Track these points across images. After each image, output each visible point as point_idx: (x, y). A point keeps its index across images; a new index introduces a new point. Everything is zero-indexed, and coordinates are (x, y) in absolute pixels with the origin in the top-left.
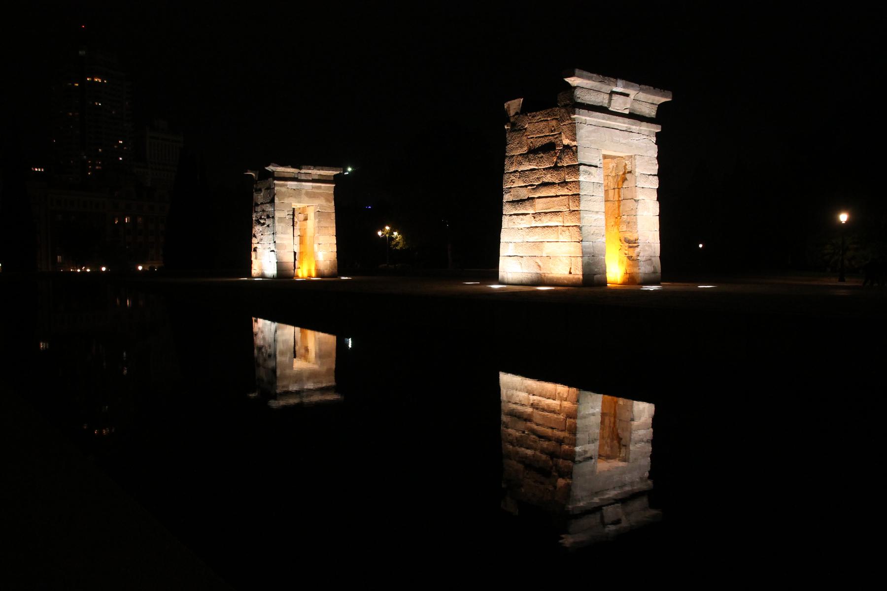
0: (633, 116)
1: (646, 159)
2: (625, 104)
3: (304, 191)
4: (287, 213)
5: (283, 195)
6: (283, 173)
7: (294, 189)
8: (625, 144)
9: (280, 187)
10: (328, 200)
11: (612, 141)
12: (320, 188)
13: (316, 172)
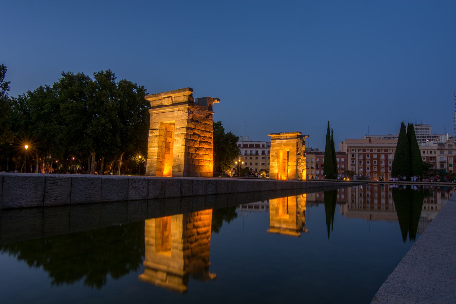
0: (175, 104)
1: (181, 121)
2: (169, 101)
4: (275, 153)
5: (274, 146)
6: (274, 137)
7: (279, 143)
8: (171, 117)
9: (273, 143)
10: (293, 146)
11: (165, 118)
12: (289, 141)
13: (288, 135)
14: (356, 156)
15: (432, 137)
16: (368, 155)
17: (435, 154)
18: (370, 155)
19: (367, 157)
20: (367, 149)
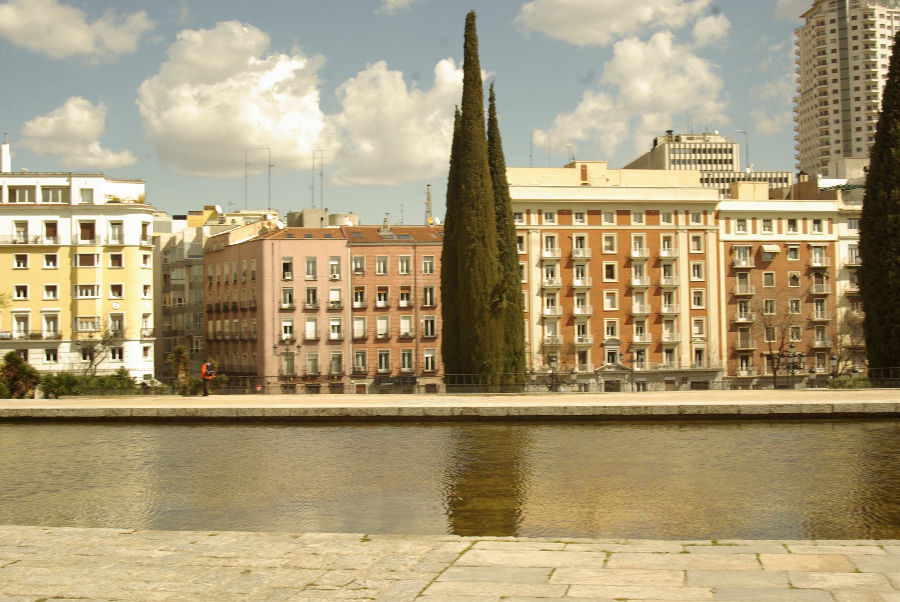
16: (581, 239)
17: (830, 231)
19: (577, 247)
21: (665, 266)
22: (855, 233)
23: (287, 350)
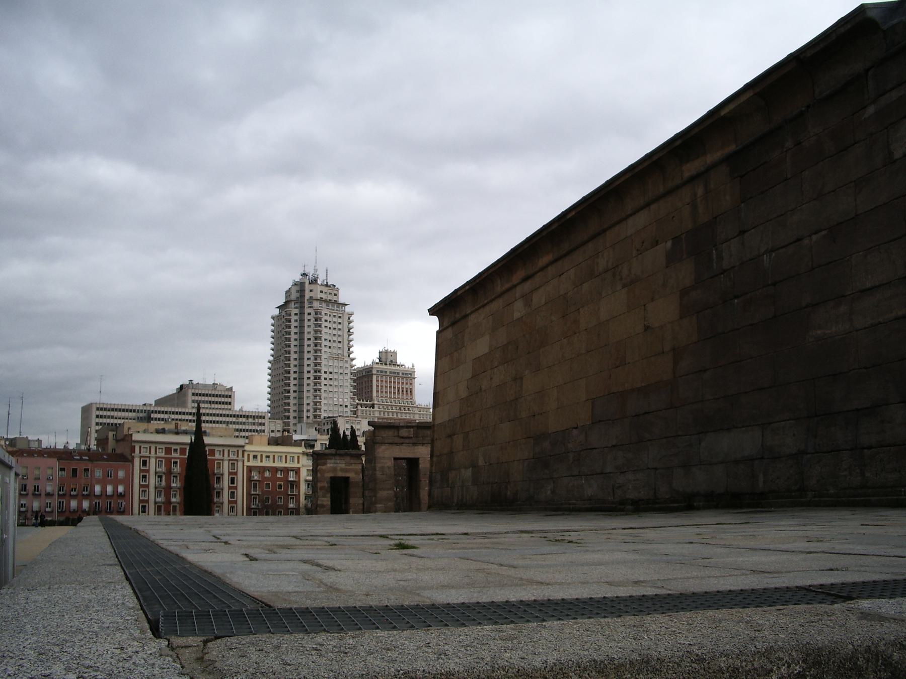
3: (338, 468)
14: (152, 463)
15: (238, 416)
16: (176, 463)
17: (298, 463)
18: (180, 463)
20: (174, 447)
21: (217, 478)
22: (310, 463)
23: (26, 516)
